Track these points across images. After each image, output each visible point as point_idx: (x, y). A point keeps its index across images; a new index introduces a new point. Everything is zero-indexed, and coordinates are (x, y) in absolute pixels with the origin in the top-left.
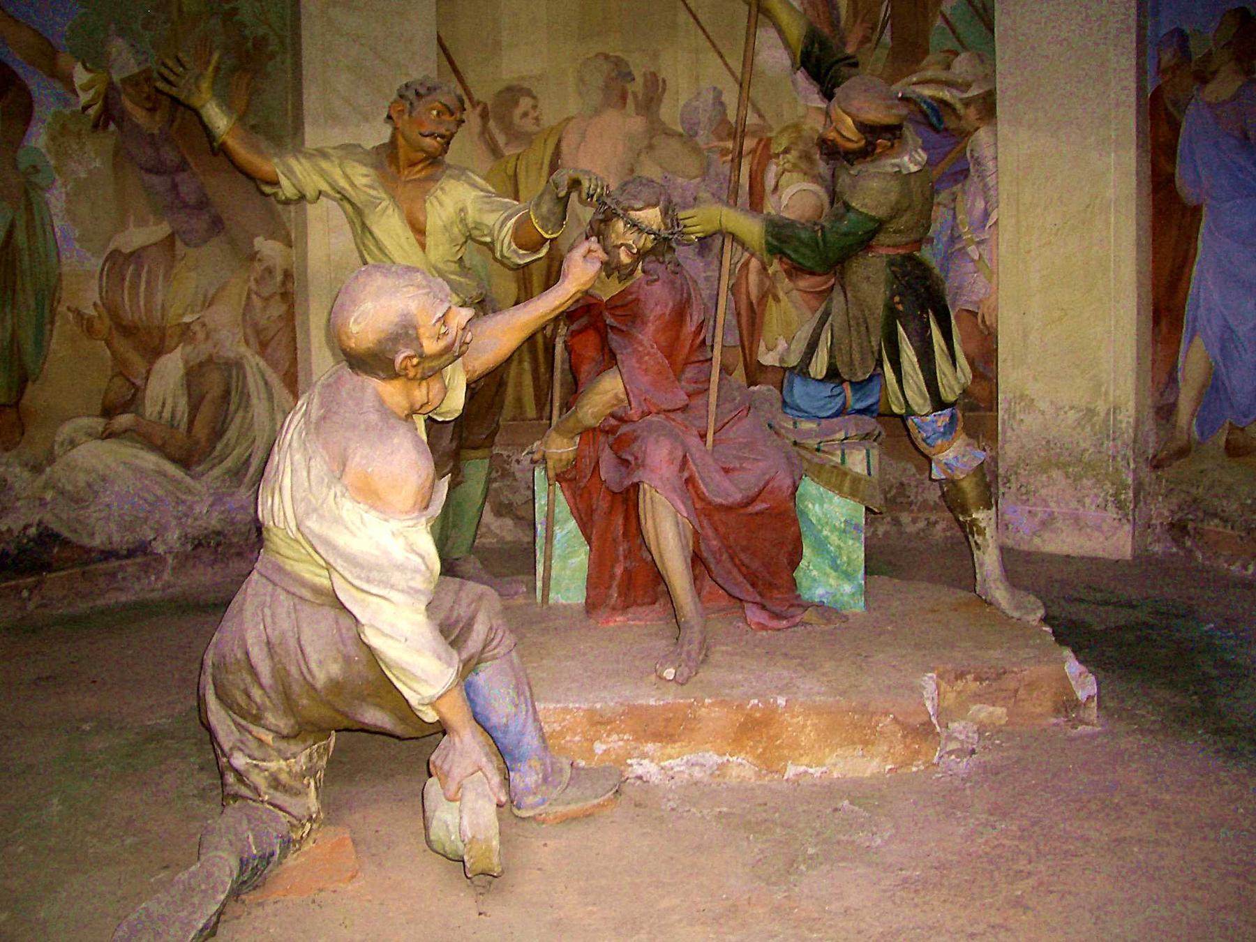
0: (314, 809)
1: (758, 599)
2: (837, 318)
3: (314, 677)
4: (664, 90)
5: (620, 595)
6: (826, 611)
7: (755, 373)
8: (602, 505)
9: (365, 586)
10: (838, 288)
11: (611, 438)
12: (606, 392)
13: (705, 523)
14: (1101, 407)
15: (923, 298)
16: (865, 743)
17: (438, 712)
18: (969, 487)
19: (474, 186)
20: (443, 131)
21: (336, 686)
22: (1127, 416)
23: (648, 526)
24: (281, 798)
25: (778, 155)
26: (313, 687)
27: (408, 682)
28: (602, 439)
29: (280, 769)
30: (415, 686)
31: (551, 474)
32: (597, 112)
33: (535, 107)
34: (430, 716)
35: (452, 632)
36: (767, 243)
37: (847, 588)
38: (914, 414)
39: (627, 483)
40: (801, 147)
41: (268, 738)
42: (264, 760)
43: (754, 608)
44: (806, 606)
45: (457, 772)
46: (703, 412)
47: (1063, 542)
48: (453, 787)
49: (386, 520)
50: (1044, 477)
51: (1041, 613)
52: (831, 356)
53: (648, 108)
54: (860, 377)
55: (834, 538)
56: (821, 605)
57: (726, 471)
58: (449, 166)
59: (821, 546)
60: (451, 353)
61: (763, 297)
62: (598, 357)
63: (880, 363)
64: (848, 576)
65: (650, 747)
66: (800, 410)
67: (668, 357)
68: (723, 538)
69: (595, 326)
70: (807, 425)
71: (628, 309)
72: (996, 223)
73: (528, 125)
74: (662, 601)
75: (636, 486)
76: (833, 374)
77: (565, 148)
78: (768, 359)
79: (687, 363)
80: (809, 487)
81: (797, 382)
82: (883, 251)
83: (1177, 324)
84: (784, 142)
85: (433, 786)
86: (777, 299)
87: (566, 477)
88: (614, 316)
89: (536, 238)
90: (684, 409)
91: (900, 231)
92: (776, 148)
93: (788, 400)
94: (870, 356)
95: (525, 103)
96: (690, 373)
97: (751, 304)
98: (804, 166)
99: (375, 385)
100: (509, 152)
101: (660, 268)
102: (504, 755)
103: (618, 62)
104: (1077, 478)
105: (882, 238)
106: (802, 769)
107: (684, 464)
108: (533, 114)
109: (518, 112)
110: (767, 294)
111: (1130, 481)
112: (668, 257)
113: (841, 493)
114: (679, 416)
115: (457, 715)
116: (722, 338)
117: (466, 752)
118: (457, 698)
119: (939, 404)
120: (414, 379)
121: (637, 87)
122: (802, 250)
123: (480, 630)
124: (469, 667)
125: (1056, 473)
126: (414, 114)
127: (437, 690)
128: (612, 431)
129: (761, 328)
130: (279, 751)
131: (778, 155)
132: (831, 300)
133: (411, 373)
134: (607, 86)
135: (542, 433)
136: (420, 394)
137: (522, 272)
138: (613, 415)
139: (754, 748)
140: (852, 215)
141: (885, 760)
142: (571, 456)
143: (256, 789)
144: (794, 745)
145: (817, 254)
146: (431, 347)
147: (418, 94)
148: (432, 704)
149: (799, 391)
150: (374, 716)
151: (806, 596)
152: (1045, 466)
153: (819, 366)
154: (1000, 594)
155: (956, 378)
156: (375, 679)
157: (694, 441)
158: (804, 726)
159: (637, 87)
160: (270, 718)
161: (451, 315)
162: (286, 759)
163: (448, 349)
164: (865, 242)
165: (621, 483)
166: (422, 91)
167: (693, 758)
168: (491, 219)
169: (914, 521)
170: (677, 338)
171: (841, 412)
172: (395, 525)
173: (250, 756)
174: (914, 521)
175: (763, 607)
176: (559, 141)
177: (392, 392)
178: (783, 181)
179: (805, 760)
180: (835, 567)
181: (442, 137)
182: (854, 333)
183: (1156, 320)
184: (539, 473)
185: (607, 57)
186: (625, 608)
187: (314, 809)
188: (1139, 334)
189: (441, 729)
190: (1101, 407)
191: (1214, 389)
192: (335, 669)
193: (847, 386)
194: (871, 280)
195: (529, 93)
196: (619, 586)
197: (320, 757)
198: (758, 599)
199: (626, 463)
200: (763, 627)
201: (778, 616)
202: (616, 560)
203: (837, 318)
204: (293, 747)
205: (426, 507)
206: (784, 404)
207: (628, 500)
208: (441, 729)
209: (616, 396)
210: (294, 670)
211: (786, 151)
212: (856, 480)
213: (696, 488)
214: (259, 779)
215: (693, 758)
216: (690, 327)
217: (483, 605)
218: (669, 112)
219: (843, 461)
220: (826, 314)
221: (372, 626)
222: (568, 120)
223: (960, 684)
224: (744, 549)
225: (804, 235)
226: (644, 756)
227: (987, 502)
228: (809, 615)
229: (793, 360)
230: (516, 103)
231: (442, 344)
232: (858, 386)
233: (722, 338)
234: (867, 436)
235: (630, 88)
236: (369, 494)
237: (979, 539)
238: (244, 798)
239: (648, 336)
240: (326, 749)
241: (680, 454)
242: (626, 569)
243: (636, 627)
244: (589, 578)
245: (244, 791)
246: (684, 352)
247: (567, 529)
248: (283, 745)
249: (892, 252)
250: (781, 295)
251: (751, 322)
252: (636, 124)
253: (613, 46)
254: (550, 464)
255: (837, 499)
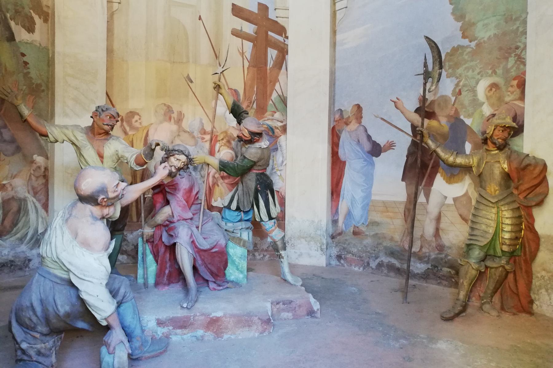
0: (54, 362)
1: (214, 280)
2: (240, 191)
3: (59, 311)
4: (184, 117)
5: (167, 280)
6: (236, 284)
7: (211, 208)
8: (162, 250)
9: (83, 278)
10: (240, 182)
11: (167, 228)
12: (165, 213)
13: (197, 255)
14: (316, 221)
15: (266, 186)
16: (249, 326)
17: (107, 321)
18: (279, 244)
19: (122, 143)
20: (111, 124)
21: (68, 315)
22: (324, 223)
23: (179, 257)
24: (41, 359)
25: (219, 141)
26: (59, 316)
27: (97, 312)
28: (163, 229)
29: (42, 348)
30: (100, 313)
31: (145, 240)
32: (161, 122)
33: (140, 119)
34: (104, 323)
35: (114, 293)
36: (220, 168)
37: (241, 276)
38: (263, 221)
39: (172, 242)
40: (227, 138)
41: (38, 335)
42: (35, 344)
43: (212, 283)
44: (228, 282)
45: (113, 344)
46: (198, 220)
47: (305, 261)
48: (111, 349)
49: (92, 254)
50: (299, 241)
51: (301, 283)
52: (238, 203)
53: (178, 123)
54: (247, 210)
55: (237, 260)
56: (232, 282)
57: (205, 238)
58: (113, 136)
59: (233, 262)
60: (118, 198)
61: (214, 184)
62: (162, 202)
63: (253, 206)
64: (242, 272)
65: (179, 331)
66: (227, 220)
67: (187, 202)
68: (203, 260)
69: (163, 192)
70: (230, 225)
71: (174, 187)
72: (286, 164)
73: (137, 125)
74: (181, 281)
75: (175, 244)
76: (238, 209)
77: (150, 133)
78: (214, 204)
79: (193, 204)
80: (230, 244)
81: (227, 211)
82: (255, 171)
83: (338, 195)
84: (222, 137)
85: (104, 350)
86: (218, 185)
87: (150, 241)
88: (169, 189)
89: (143, 162)
90: (191, 219)
91: (260, 166)
92: (219, 138)
93: (224, 216)
94: (249, 203)
95: (136, 117)
96: (194, 207)
97: (210, 187)
98: (228, 144)
99: (89, 208)
100: (131, 133)
101: (185, 174)
102: (129, 336)
103: (169, 107)
104: (309, 242)
105: (255, 168)
106: (229, 336)
107: (191, 236)
108: (139, 121)
109: (134, 120)
110: (215, 184)
111: (325, 242)
112: (187, 171)
113: (240, 246)
114: (189, 221)
115: (115, 323)
116: (202, 197)
117: (117, 336)
118: (115, 315)
119: (271, 218)
120: (105, 206)
121: (175, 115)
122: (230, 170)
123: (122, 291)
124: (119, 304)
125: (303, 240)
126: (101, 117)
127: (109, 314)
128: (167, 226)
129: (213, 194)
130: (42, 341)
131: (219, 141)
132: (238, 186)
133: (104, 204)
134: (165, 114)
135: (141, 227)
136: (106, 211)
137: (134, 173)
138: (167, 220)
139: (213, 329)
140: (246, 160)
141: (255, 332)
142: (152, 233)
143: (30, 356)
144: (226, 328)
145: (234, 172)
146: (111, 195)
147: (102, 110)
148: (106, 319)
149: (227, 213)
150: (81, 325)
151: (228, 279)
152: (300, 237)
153: (234, 206)
154: (289, 277)
155: (276, 210)
156: (84, 310)
157: (194, 229)
158: (230, 321)
159: (175, 115)
160: (39, 328)
161: (119, 185)
162: (44, 343)
163: (117, 196)
164: (249, 169)
165: (169, 242)
166: (104, 109)
167: (193, 334)
168: (127, 155)
169: (259, 255)
170: (190, 196)
171: (241, 220)
172: (96, 255)
173: (29, 344)
174: (259, 255)
175: (215, 282)
176: (148, 131)
177: (96, 210)
178: (221, 149)
179: (230, 333)
180: (238, 269)
181: (111, 126)
182: (245, 196)
183: (332, 194)
184: (140, 240)
185: (165, 104)
186: (169, 284)
187: (54, 362)
188: (327, 198)
189: (108, 328)
190: (316, 221)
191: (349, 214)
192: (67, 308)
193: (242, 213)
194: (251, 180)
195: (138, 114)
196: (167, 277)
197: (58, 342)
198: (214, 280)
199: (172, 236)
200: (215, 289)
201: (219, 286)
202: (166, 268)
203: (240, 191)
204: (48, 338)
205: (107, 249)
206: (222, 218)
207: (172, 248)
208: (108, 328)
209: (169, 215)
210: (51, 309)
211: (222, 139)
212: (245, 241)
213: (195, 244)
214: (32, 353)
215: (193, 334)
216: (194, 193)
217: (123, 285)
218: (185, 124)
219: (241, 235)
220: (237, 190)
221: (85, 292)
222: (152, 124)
223: (278, 306)
224: (209, 264)
225: (231, 165)
226: (176, 334)
227: (285, 249)
228: (229, 285)
229: (226, 204)
230: (133, 117)
231: (116, 194)
232: (246, 213)
233: (202, 197)
234: (247, 228)
235: (173, 115)
236: (86, 244)
237: (282, 260)
238: (25, 360)
239: (180, 195)
240: (61, 338)
241: (190, 233)
242: (169, 271)
243: (176, 289)
244: (157, 274)
245: (25, 358)
246: (191, 200)
247: (150, 258)
248: (43, 338)
249: (257, 172)
250: (219, 184)
251: (210, 192)
252: (174, 127)
253: (168, 102)
254: (145, 236)
255: (238, 247)
